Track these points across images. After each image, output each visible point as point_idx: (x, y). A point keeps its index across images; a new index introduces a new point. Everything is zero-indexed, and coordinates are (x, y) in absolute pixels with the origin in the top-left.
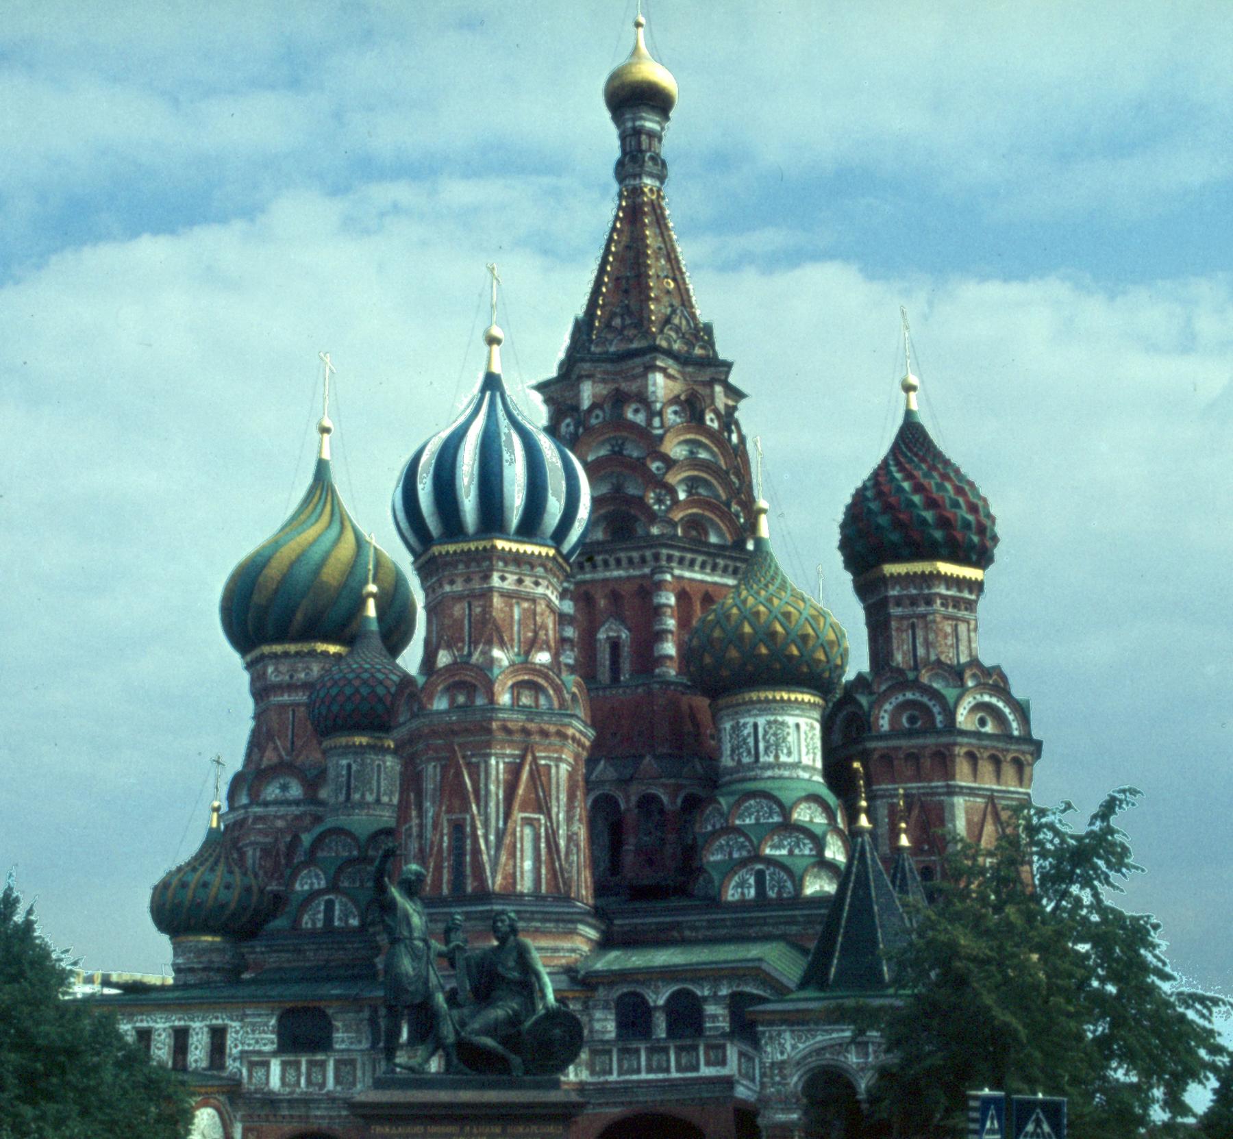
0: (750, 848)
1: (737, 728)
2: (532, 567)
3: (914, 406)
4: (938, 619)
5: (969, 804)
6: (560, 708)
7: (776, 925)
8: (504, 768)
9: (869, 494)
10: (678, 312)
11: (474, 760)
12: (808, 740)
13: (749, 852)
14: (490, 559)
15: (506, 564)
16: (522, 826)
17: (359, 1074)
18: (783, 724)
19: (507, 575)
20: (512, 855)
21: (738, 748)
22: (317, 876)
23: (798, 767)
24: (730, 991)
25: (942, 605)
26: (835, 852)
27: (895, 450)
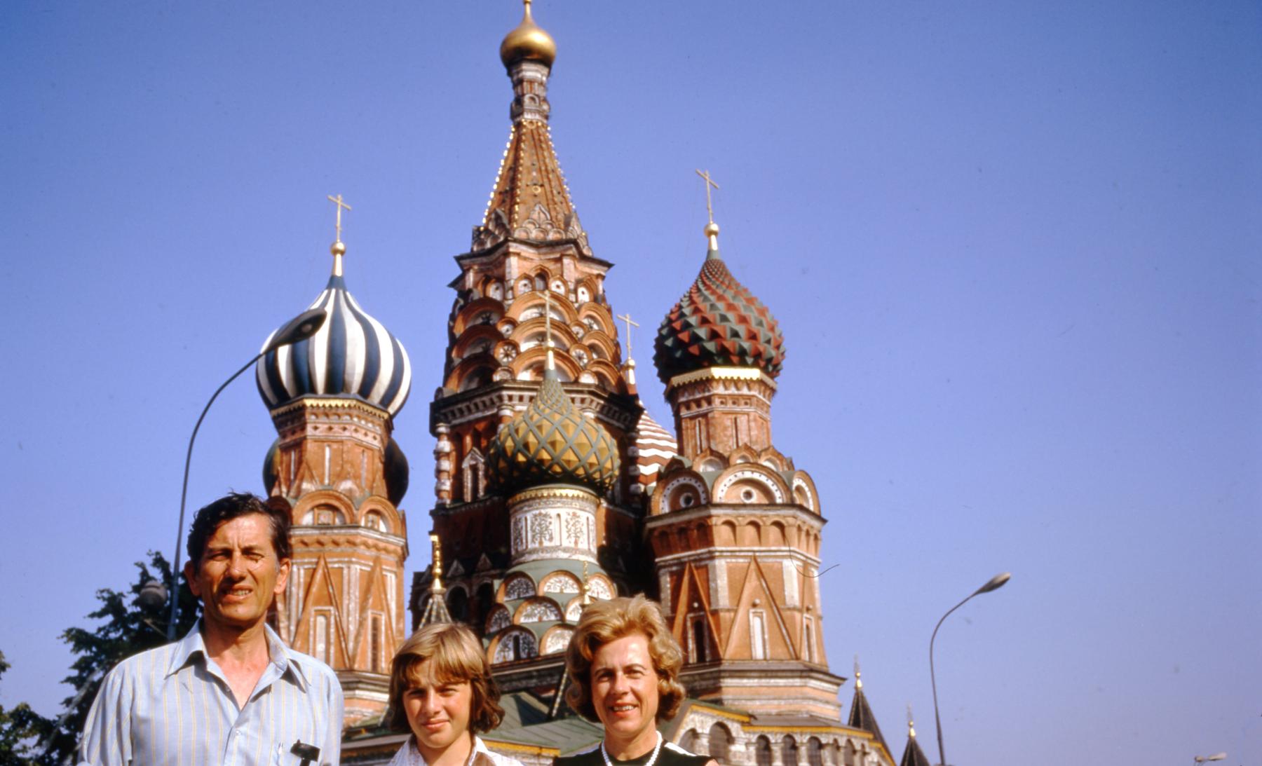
3: (715, 246)
4: (717, 416)
5: (731, 565)
6: (351, 523)
7: (519, 680)
8: (305, 574)
12: (569, 527)
14: (303, 415)
15: (317, 416)
16: (315, 617)
18: (546, 515)
19: (318, 425)
23: (559, 549)
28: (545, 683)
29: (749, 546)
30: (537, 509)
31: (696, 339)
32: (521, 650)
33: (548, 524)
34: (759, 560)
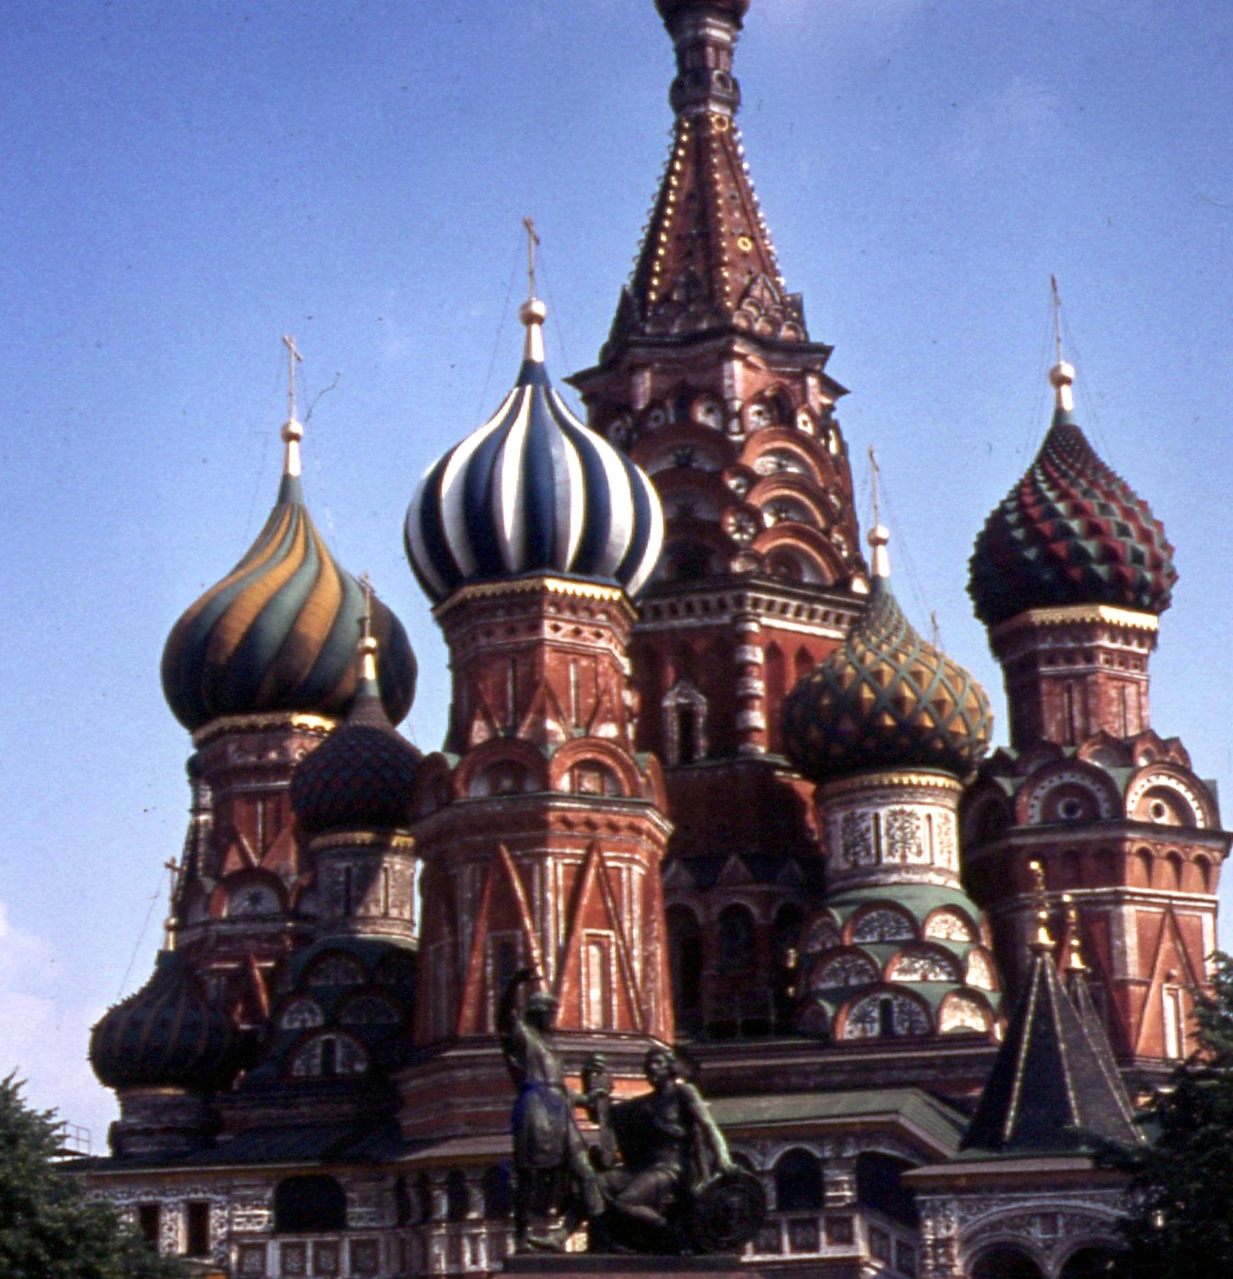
0: (872, 972)
1: (851, 821)
2: (592, 613)
3: (1068, 404)
4: (1101, 681)
5: (1142, 914)
6: (632, 796)
9: (1012, 518)
10: (759, 281)
11: (526, 861)
13: (871, 977)
14: (539, 604)
15: (559, 610)
17: (382, 1258)
18: (911, 814)
19: (561, 624)
20: (577, 982)
21: (855, 845)
22: (311, 1011)
23: (932, 870)
24: (857, 1152)
25: (1107, 661)
26: (979, 975)
27: (1044, 459)
28: (951, 1076)
29: (1164, 889)
30: (898, 803)
31: (1080, 555)
32: (895, 1022)
33: (914, 827)
34: (1177, 911)
